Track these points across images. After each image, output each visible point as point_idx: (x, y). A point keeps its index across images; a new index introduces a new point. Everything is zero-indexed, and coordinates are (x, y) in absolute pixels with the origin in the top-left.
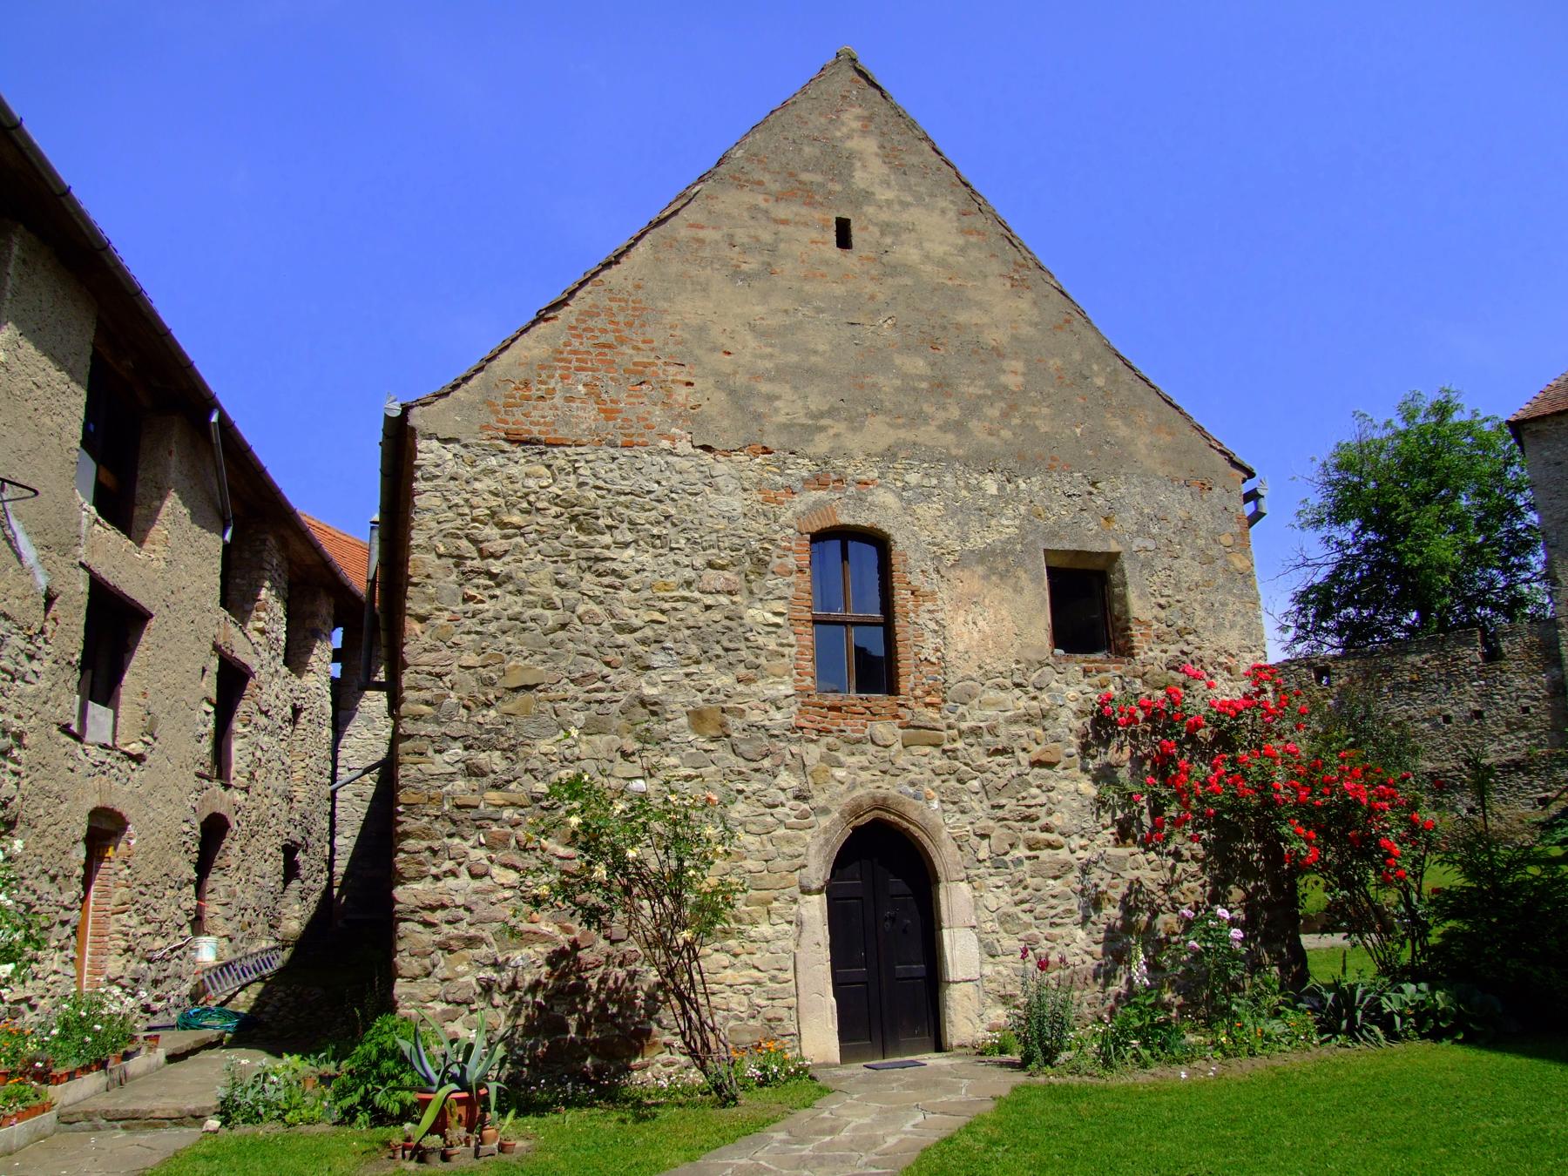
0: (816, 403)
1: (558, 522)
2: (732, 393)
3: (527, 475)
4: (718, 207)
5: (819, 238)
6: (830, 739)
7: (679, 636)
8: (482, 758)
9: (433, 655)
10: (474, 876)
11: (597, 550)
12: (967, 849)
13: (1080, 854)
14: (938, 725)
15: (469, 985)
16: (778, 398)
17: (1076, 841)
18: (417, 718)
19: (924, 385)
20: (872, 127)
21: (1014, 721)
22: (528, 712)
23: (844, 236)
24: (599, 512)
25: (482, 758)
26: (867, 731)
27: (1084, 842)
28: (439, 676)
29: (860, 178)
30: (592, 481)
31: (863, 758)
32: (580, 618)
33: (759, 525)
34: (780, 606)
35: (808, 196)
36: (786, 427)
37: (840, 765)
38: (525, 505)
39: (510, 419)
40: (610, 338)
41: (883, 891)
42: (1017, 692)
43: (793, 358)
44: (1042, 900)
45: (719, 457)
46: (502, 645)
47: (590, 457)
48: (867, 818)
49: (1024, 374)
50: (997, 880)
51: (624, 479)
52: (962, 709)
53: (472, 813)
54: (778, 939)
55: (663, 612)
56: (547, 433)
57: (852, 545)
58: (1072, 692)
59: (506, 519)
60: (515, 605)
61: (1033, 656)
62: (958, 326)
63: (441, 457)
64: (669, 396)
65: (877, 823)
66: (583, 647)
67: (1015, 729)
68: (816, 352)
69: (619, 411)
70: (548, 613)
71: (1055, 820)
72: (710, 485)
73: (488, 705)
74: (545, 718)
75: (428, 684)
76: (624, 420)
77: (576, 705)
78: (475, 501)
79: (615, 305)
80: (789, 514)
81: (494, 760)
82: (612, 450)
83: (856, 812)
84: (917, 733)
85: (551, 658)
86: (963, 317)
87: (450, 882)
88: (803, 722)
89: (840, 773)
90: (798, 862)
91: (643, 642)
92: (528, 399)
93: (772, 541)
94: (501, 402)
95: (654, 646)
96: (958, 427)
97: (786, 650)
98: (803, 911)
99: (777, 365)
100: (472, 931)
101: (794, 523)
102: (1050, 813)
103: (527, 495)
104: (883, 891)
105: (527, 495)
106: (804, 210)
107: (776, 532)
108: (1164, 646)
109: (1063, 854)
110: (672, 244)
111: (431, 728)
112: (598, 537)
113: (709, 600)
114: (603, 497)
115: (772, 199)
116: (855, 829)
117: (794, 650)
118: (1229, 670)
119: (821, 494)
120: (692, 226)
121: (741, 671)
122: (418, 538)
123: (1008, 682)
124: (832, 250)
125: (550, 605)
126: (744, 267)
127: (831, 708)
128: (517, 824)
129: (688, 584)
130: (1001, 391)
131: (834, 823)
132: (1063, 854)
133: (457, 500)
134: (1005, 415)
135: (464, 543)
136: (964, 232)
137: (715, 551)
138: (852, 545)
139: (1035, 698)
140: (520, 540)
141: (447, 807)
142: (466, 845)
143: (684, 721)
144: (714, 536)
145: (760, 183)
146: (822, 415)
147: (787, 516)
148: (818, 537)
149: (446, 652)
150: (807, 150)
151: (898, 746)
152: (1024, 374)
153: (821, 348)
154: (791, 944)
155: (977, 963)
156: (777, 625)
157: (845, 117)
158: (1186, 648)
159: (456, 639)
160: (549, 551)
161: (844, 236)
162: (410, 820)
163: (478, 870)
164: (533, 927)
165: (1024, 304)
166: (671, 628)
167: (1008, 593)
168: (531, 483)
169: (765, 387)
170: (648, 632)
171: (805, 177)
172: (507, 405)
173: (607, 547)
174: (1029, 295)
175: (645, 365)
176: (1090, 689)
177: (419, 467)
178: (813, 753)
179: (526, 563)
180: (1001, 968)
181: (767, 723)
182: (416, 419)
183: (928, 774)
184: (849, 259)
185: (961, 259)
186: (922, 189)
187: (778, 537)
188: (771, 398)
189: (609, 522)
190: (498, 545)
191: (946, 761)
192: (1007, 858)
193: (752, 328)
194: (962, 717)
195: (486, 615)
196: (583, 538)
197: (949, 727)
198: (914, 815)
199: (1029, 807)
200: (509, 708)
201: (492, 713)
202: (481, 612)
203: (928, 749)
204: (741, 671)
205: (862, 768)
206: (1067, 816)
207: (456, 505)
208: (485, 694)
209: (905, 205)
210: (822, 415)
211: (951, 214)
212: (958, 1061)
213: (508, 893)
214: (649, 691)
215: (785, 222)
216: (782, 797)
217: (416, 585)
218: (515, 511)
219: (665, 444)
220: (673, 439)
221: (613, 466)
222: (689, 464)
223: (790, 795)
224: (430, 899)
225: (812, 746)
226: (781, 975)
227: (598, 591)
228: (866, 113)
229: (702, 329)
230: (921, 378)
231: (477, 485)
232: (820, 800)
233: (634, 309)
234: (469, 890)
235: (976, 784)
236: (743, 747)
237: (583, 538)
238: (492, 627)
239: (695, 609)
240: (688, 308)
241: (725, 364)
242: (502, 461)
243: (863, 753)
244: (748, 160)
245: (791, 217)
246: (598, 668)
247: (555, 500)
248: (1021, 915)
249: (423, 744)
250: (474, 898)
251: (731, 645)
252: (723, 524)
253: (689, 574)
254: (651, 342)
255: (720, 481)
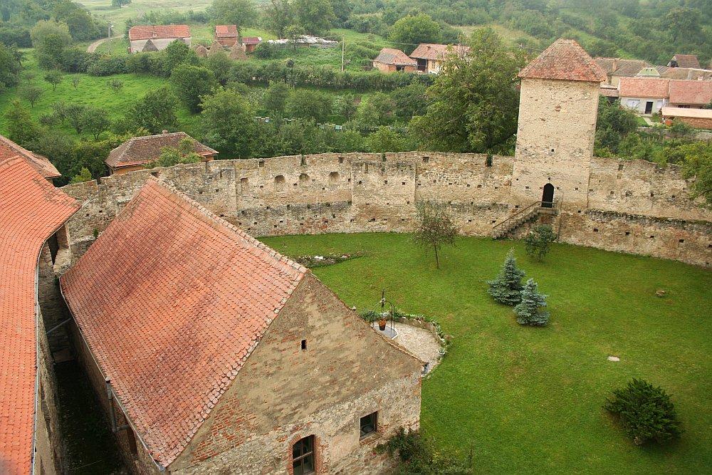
0: (294, 404)
2: (268, 414)
4: (260, 354)
19: (328, 384)
23: (304, 346)
29: (310, 322)
35: (292, 337)
40: (228, 415)
43: (287, 394)
62: (340, 359)
96: (339, 393)
126: (271, 372)
134: (352, 382)
146: (296, 408)
147: (286, 443)
161: (304, 346)
165: (363, 342)
169: (278, 408)
171: (291, 330)
174: (364, 338)
184: (307, 353)
188: (280, 410)
193: (274, 391)
209: (325, 325)
210: (296, 408)
219: (249, 439)
228: (314, 294)
230: (327, 382)
240: (253, 394)
241: (265, 406)
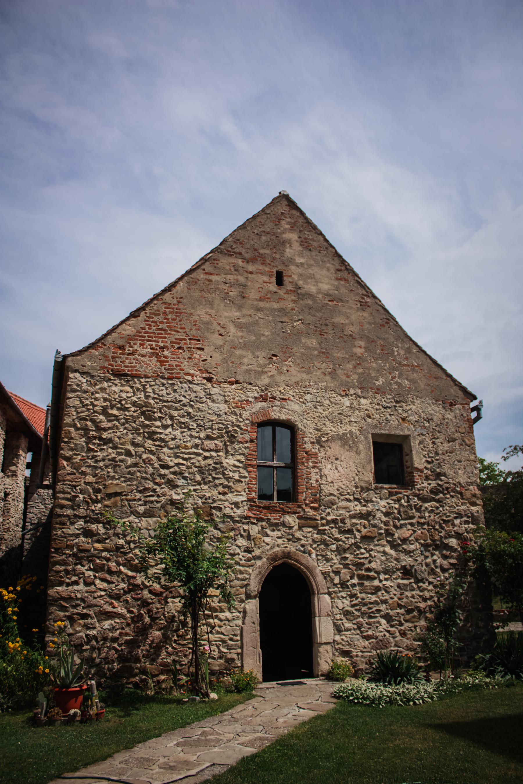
1: (135, 414)
3: (121, 391)
5: (268, 281)
6: (264, 523)
7: (191, 470)
8: (94, 527)
9: (72, 476)
10: (87, 584)
11: (153, 428)
12: (328, 578)
13: (384, 582)
14: (317, 517)
15: (82, 637)
16: (244, 357)
17: (382, 576)
18: (62, 507)
19: (316, 352)
20: (295, 228)
21: (352, 517)
22: (116, 506)
24: (155, 410)
25: (94, 527)
26: (282, 520)
27: (387, 576)
28: (75, 486)
30: (152, 395)
31: (279, 533)
32: (144, 461)
33: (233, 418)
34: (242, 458)
36: (248, 371)
37: (267, 535)
38: (119, 406)
39: (115, 364)
40: (164, 326)
41: (286, 598)
42: (356, 503)
44: (365, 605)
45: (215, 385)
46: (106, 473)
47: (153, 383)
48: (280, 562)
49: (365, 348)
50: (343, 594)
51: (168, 394)
52: (328, 510)
53: (87, 554)
54: (234, 619)
55: (184, 459)
56: (132, 371)
57: (278, 429)
58: (383, 503)
59: (111, 412)
60: (112, 453)
61: (363, 485)
63: (80, 381)
64: (192, 355)
65: (285, 565)
66: (144, 475)
67: (355, 521)
68: (263, 335)
69: (167, 362)
70: (128, 458)
71: (373, 565)
72: (210, 398)
73: (97, 501)
74: (125, 508)
75: (69, 490)
76: (170, 365)
77: (141, 503)
78: (96, 403)
79: (168, 310)
80: (248, 413)
81: (100, 528)
82: (163, 381)
83: (274, 558)
84: (306, 521)
85: (129, 480)
86: (336, 320)
87: (76, 587)
88: (250, 514)
89: (267, 540)
90: (246, 582)
91: (174, 473)
92: (123, 354)
93: (239, 427)
94: (110, 355)
95: (179, 476)
97: (243, 480)
98: (247, 606)
99: (244, 341)
100: (85, 611)
101: (250, 418)
102: (370, 562)
103: (121, 400)
104: (286, 598)
105: (121, 400)
106: (261, 267)
107: (240, 422)
108: (430, 482)
109: (376, 583)
110: (196, 282)
111: (69, 512)
112: (154, 422)
113: (207, 454)
114: (157, 403)
115: (245, 261)
116: (274, 567)
117: (247, 480)
118: (461, 493)
119: (263, 404)
120: (206, 273)
121: (221, 489)
122: (68, 420)
123: (351, 498)
124: (273, 287)
125: (128, 453)
127: (264, 508)
128: (108, 560)
129: (196, 446)
130: (353, 355)
131: (263, 564)
132: (376, 583)
133: (87, 402)
135: (89, 423)
136: (337, 279)
137: (210, 430)
138: (278, 429)
139: (364, 506)
140: (115, 422)
141: (75, 550)
142: (83, 569)
143: (191, 512)
144: (210, 423)
145: (240, 254)
148: (261, 425)
149: (78, 475)
150: (263, 238)
151: (296, 527)
152: (365, 348)
153: (266, 333)
154: (240, 622)
155: (332, 635)
156: (238, 467)
157: (283, 222)
158: (440, 483)
159: (83, 469)
160: (131, 428)
162: (57, 556)
163: (89, 580)
164: (115, 610)
166: (188, 467)
167: (353, 454)
168: (124, 395)
170: (176, 468)
171: (262, 251)
172: (113, 357)
173: (158, 427)
175: (181, 340)
176: (392, 502)
177: (70, 385)
178: (254, 530)
179: (118, 434)
180: (344, 637)
181: (233, 514)
182: (69, 362)
183: (310, 541)
185: (336, 292)
186: (318, 258)
187: (241, 424)
189: (160, 415)
190: (106, 424)
191: (319, 536)
192: (348, 584)
194: (329, 514)
195: (98, 458)
196: (147, 422)
197: (322, 518)
198: (303, 561)
199: (360, 558)
200: (107, 503)
201: (99, 505)
202: (96, 456)
203: (311, 529)
204: (221, 489)
205: (279, 538)
206: (379, 563)
207: (87, 405)
208: (96, 496)
209: (310, 266)
211: (333, 271)
212: (321, 682)
213: (103, 593)
214: (175, 497)
215: (251, 273)
216: (238, 551)
217: (65, 442)
218: (115, 408)
219: (190, 378)
220: (192, 375)
221: (163, 388)
222: (200, 388)
223: (242, 550)
224: (64, 595)
225: (254, 526)
226: (235, 638)
227: (153, 448)
229: (208, 323)
230: (315, 349)
231: (97, 395)
232: (257, 552)
233: (177, 313)
234: (84, 591)
235: (334, 547)
236: (221, 525)
237: (147, 422)
238: (101, 464)
239: (200, 458)
242: (110, 384)
243: (279, 530)
244: (235, 242)
245: (254, 270)
246: (151, 485)
247: (134, 404)
248: (354, 612)
249: (64, 519)
250: (86, 595)
251: (217, 476)
252: (214, 418)
253: (197, 441)
254: (184, 328)
255: (215, 397)
